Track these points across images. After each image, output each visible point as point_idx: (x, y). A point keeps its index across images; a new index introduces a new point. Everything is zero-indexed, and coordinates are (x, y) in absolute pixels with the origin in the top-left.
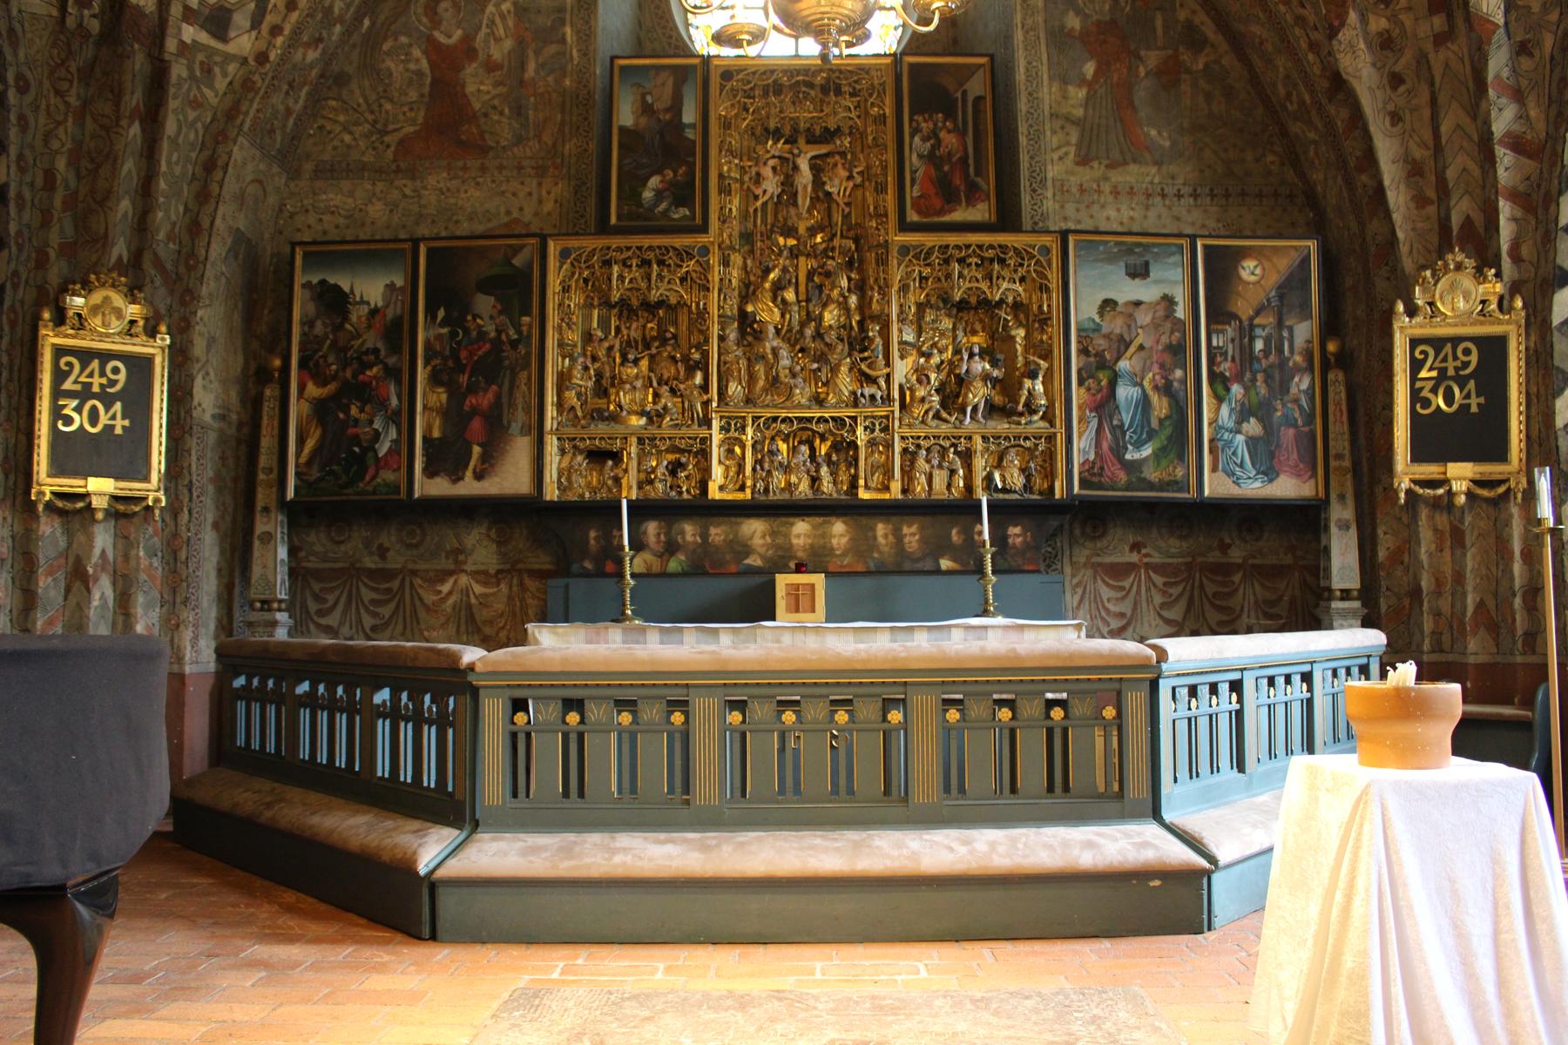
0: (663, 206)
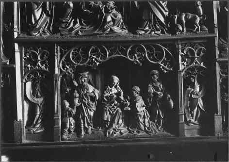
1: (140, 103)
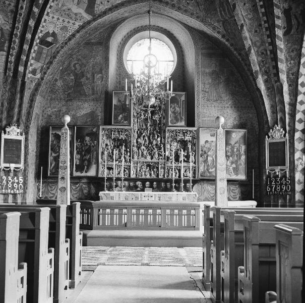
0: (122, 121)
1: (152, 172)
